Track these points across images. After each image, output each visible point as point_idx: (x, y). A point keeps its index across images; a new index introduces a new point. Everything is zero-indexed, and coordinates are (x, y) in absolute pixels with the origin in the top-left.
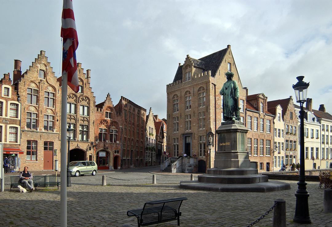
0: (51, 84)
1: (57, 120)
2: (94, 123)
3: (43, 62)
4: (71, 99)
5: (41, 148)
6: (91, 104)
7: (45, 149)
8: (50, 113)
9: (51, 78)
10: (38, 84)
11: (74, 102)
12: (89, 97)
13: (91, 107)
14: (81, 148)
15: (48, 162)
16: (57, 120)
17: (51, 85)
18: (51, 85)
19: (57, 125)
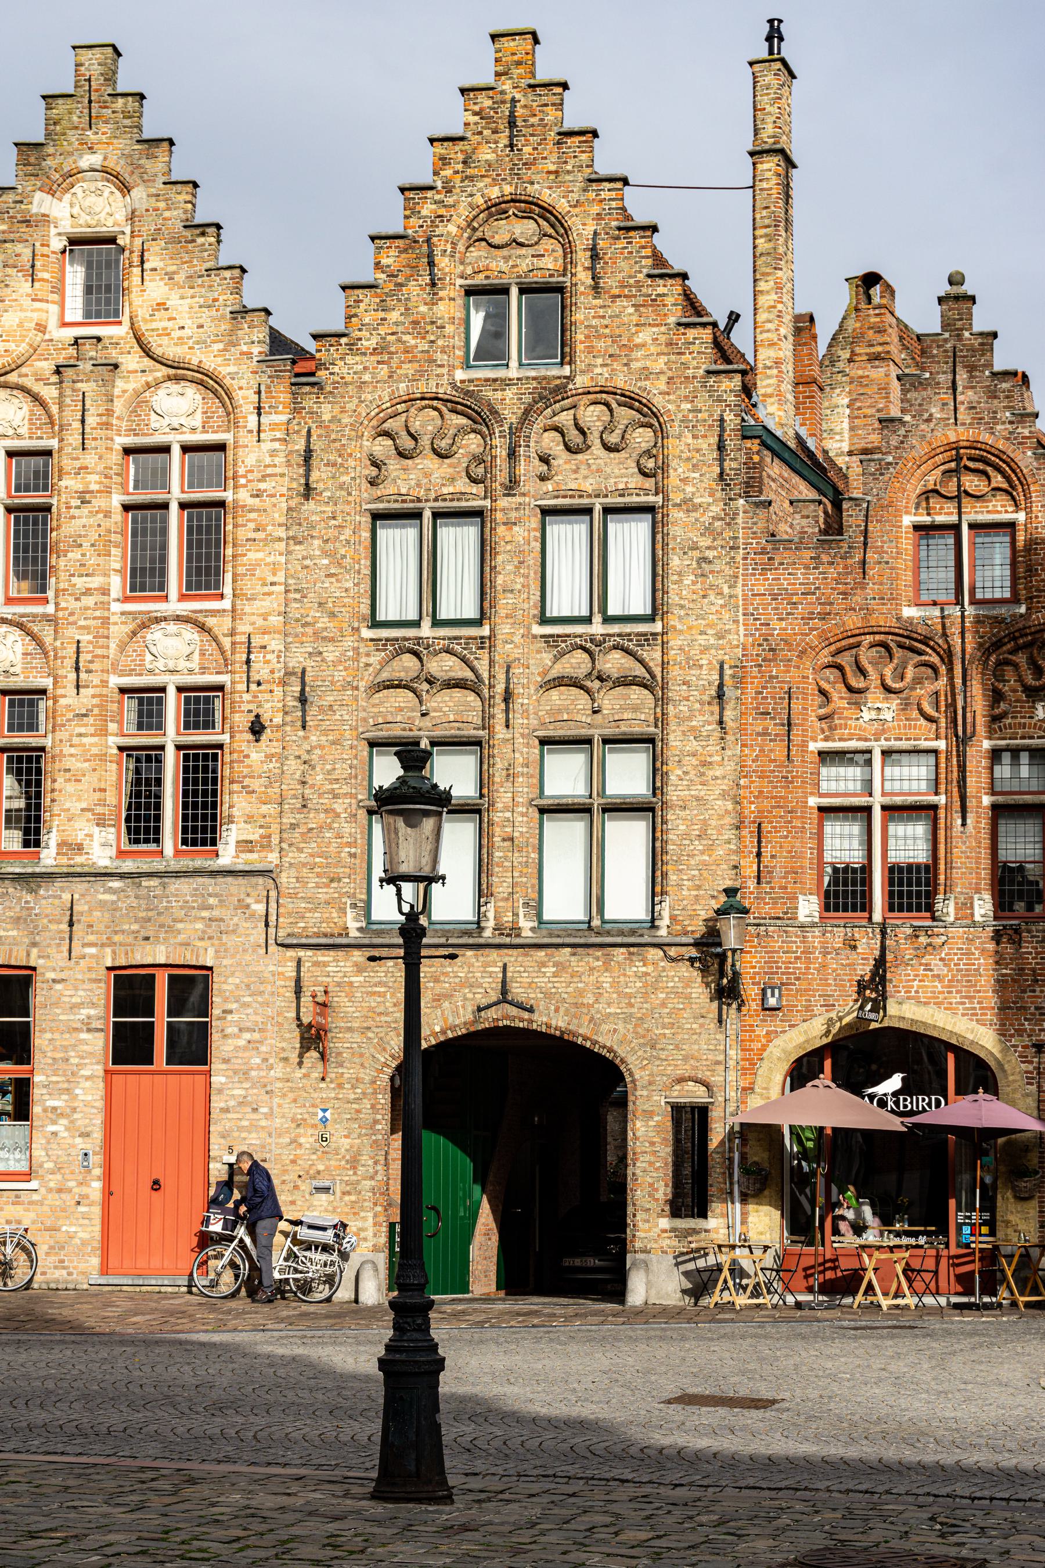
0: (170, 350)
1: (257, 729)
2: (729, 692)
3: (87, 161)
4: (428, 462)
5: (68, 1039)
6: (678, 470)
7: (130, 1046)
8: (182, 665)
9: (174, 301)
10: (49, 393)
11: (462, 485)
12: (655, 391)
13: (688, 505)
14: (550, 1018)
15: (156, 1185)
16: (257, 729)
17: (179, 372)
18: (179, 372)
19: (256, 784)
